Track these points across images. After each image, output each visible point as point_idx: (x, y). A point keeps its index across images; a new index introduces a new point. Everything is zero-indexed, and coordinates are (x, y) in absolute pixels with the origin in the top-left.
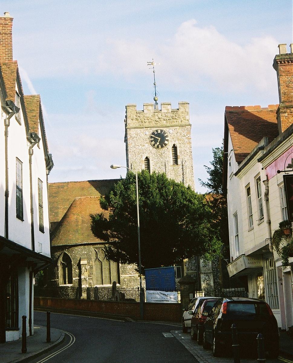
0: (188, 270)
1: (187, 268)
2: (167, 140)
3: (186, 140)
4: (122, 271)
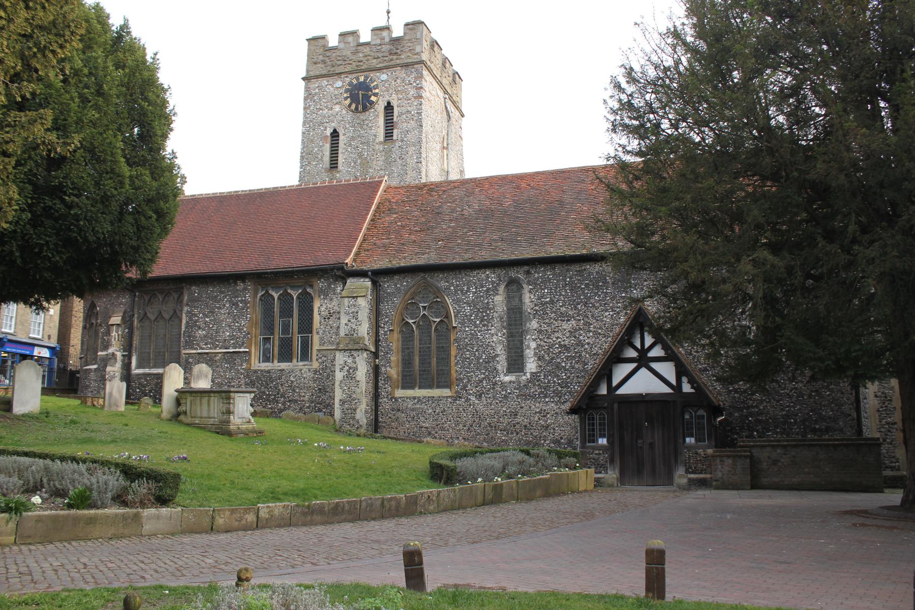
1: (321, 339)
2: (376, 95)
3: (412, 92)
4: (186, 342)
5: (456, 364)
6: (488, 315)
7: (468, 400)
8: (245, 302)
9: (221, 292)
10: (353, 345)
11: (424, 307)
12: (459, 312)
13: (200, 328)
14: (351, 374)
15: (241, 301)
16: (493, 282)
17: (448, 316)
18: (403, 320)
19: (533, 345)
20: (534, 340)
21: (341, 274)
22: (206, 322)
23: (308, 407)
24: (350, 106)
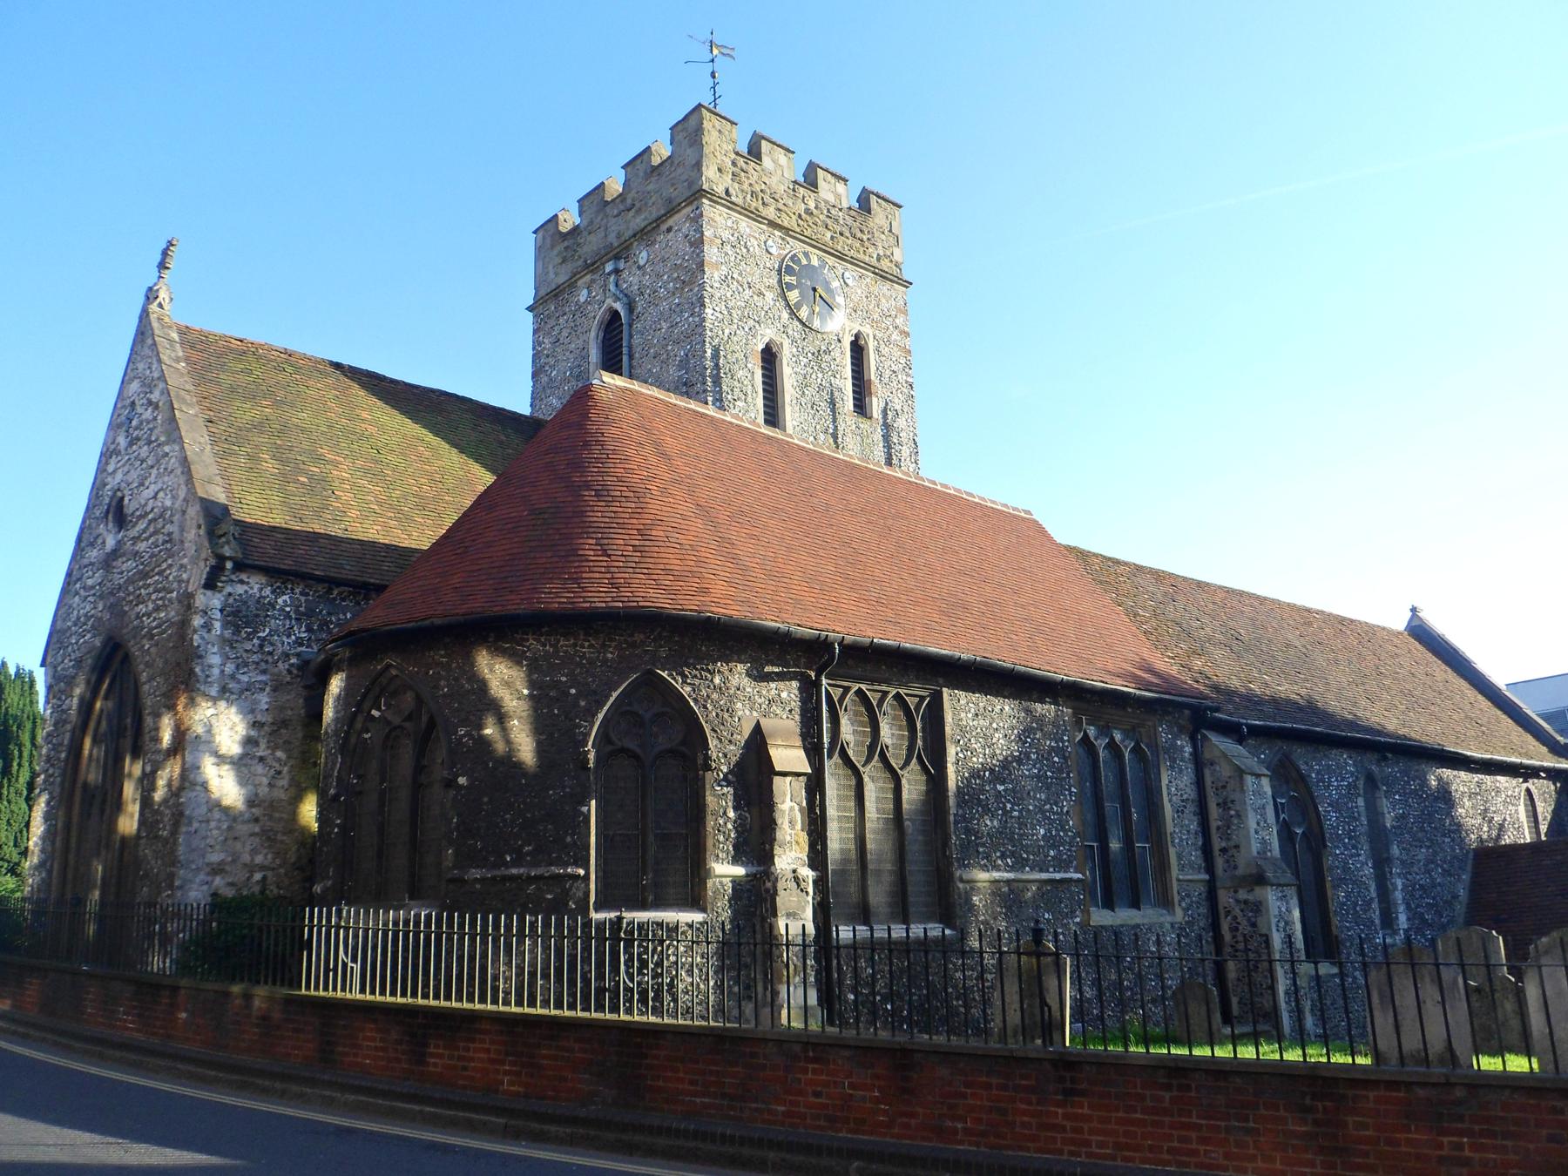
0: (1182, 868)
1: (1180, 857)
13: (987, 810)
19: (1399, 883)
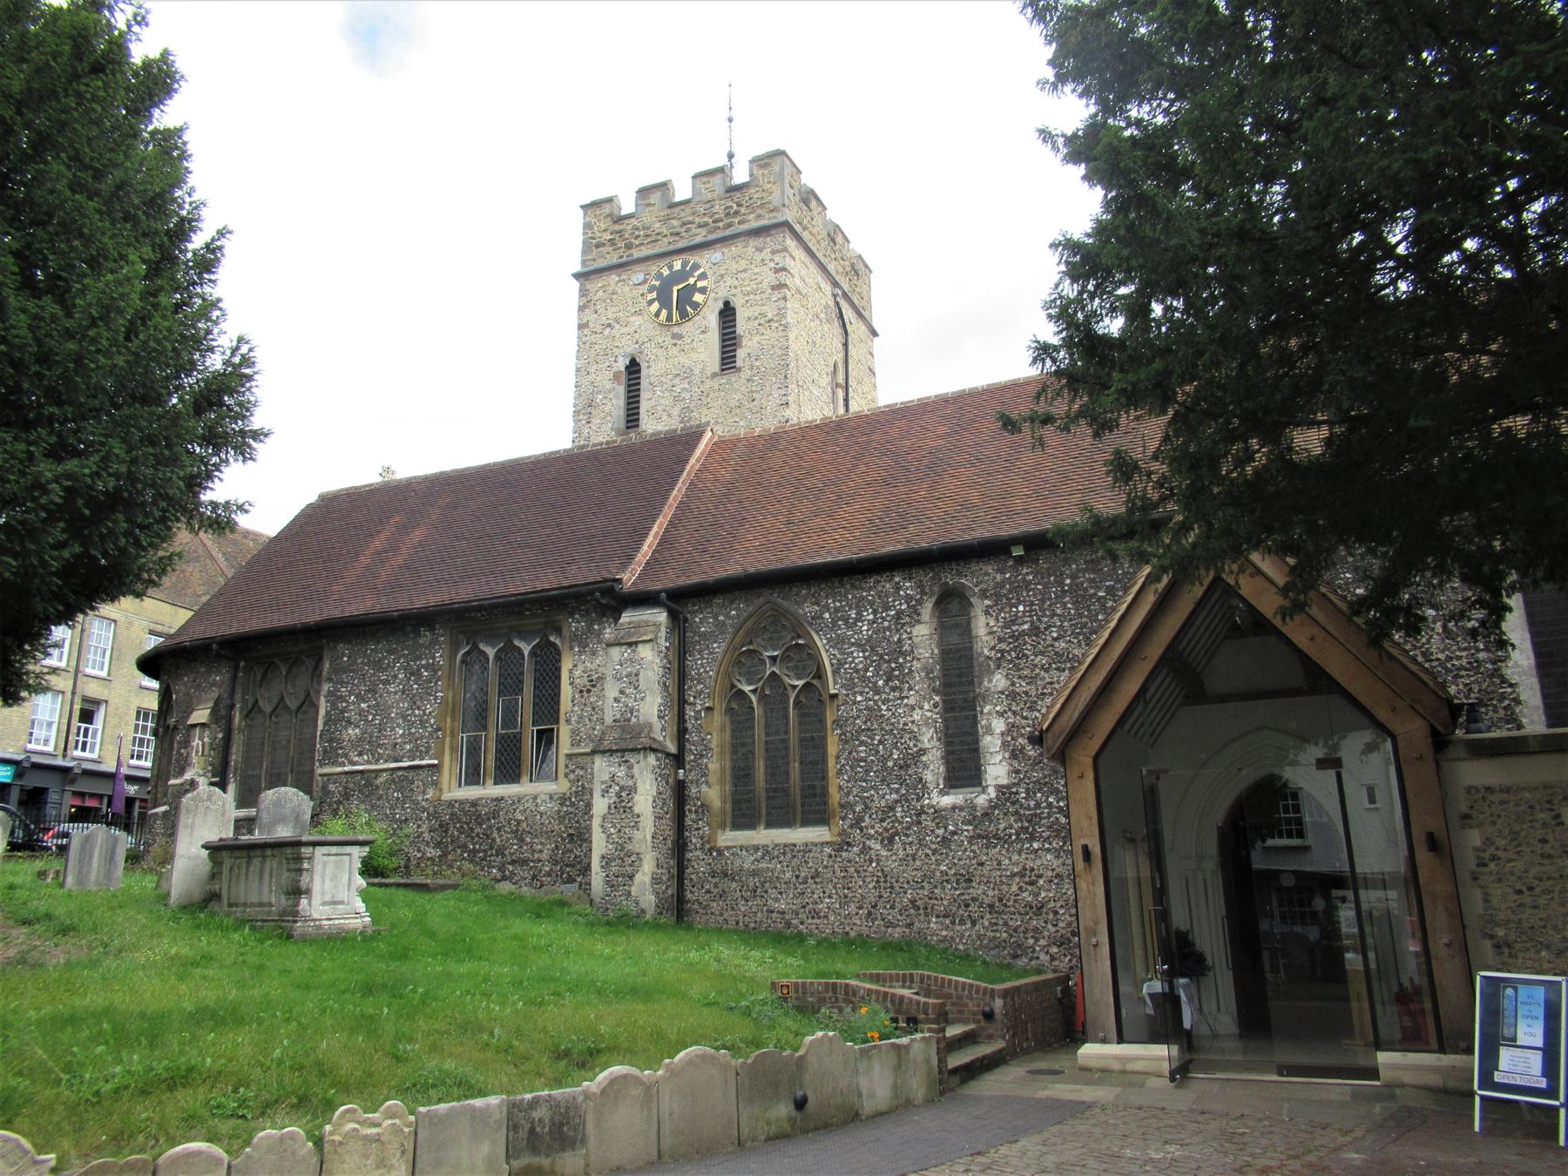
1: (575, 733)
2: (703, 290)
4: (325, 751)
5: (840, 773)
6: (900, 667)
7: (865, 850)
8: (433, 668)
9: (391, 652)
10: (627, 742)
11: (773, 659)
12: (841, 664)
13: (349, 722)
14: (622, 804)
15: (427, 667)
16: (908, 598)
17: (819, 674)
18: (733, 686)
19: (999, 725)
20: (1001, 714)
21: (608, 601)
22: (361, 712)
23: (549, 874)
24: (657, 315)
